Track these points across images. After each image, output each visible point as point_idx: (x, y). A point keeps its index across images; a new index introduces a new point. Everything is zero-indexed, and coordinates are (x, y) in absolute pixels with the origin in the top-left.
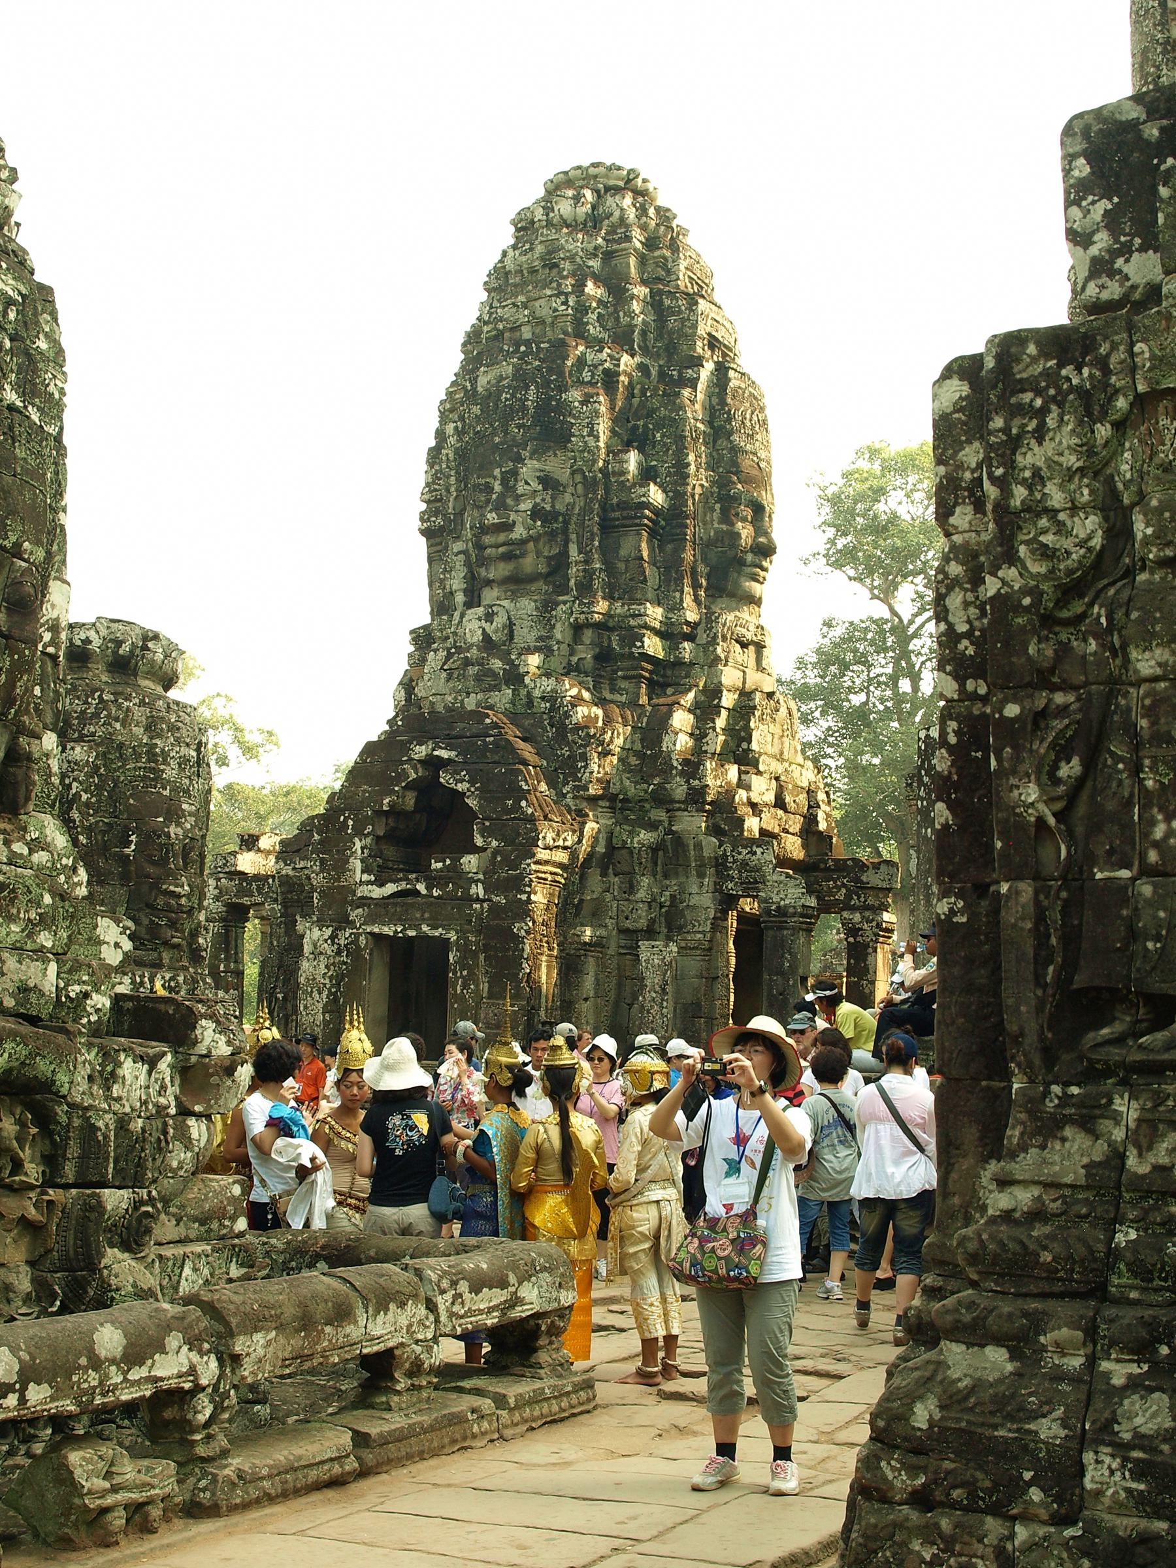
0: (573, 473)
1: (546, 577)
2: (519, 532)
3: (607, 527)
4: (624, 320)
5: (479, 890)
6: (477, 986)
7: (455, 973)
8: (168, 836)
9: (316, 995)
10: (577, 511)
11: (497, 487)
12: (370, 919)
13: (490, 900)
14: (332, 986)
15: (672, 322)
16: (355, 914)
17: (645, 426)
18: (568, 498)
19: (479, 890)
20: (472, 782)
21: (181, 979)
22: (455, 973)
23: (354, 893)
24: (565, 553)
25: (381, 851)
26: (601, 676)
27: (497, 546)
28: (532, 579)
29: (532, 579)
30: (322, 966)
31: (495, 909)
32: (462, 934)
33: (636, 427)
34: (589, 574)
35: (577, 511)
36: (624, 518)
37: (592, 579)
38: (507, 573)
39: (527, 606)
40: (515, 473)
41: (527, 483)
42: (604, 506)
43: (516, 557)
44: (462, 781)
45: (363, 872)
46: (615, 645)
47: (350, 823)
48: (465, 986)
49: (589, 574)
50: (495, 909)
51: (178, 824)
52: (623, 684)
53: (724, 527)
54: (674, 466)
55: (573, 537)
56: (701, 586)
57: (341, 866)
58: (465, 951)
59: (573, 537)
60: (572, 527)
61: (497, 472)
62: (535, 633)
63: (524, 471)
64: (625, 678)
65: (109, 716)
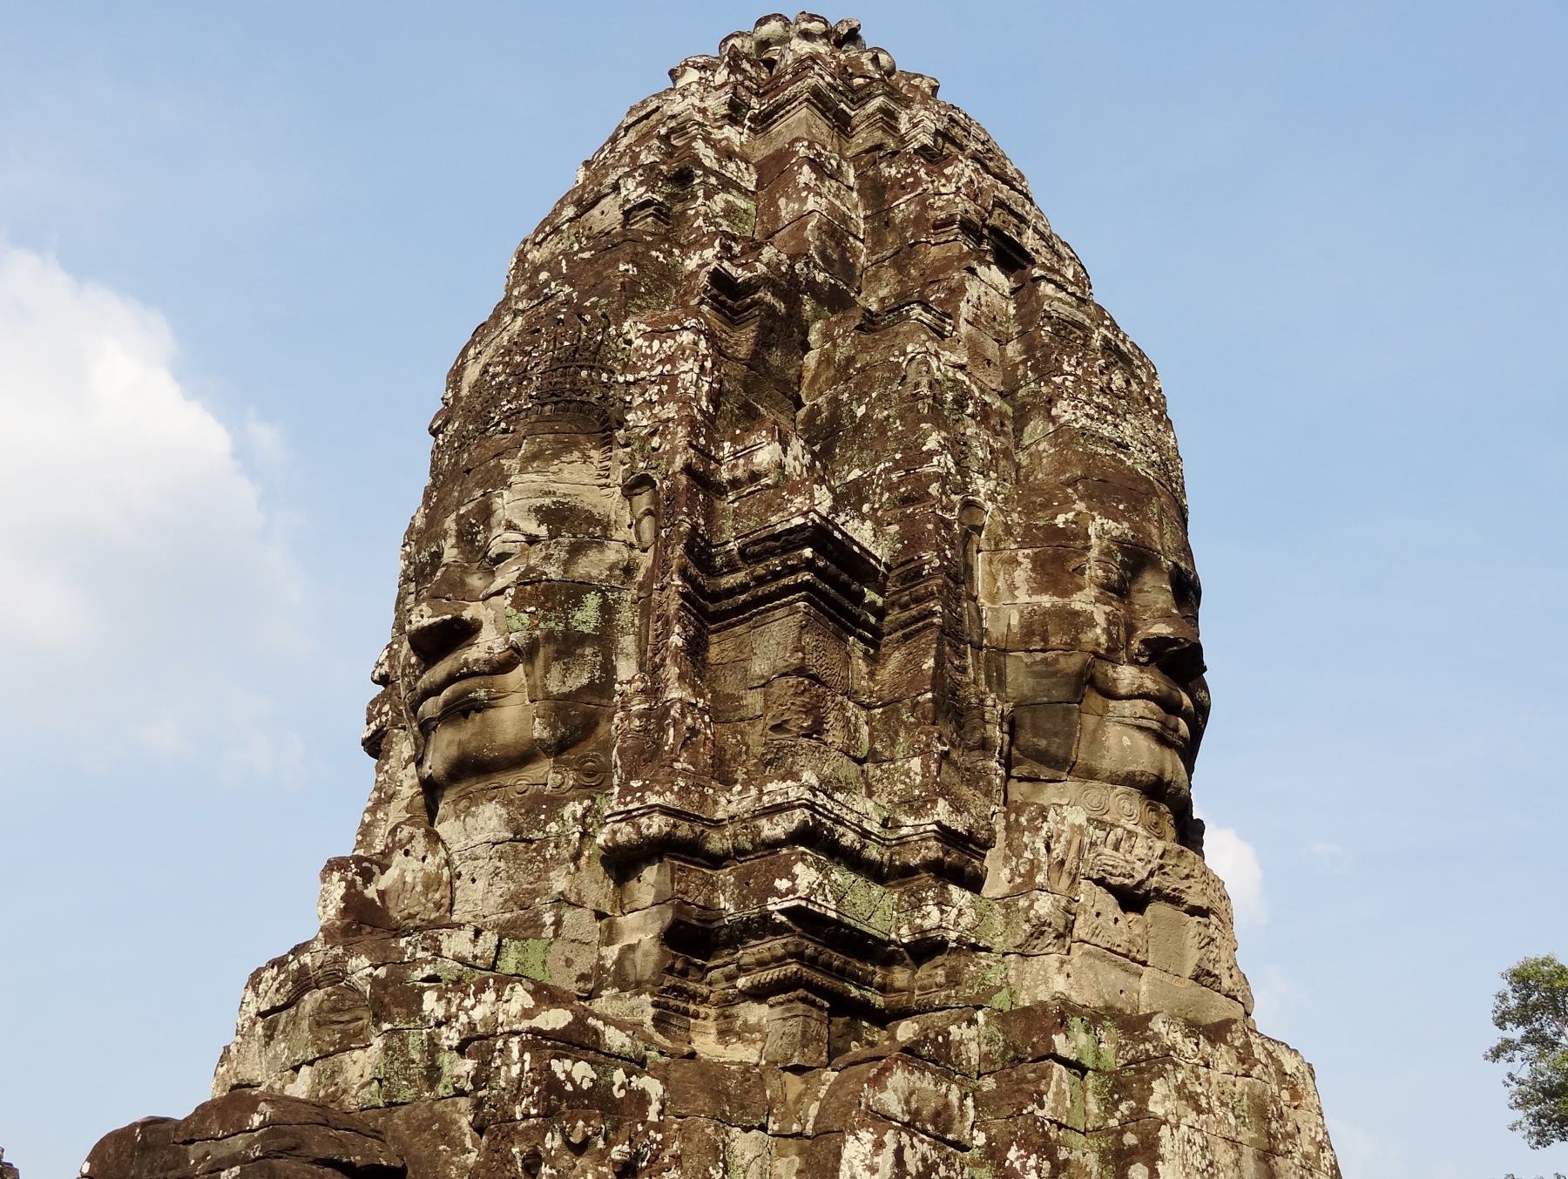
0: (631, 489)
1: (558, 749)
2: (488, 644)
3: (710, 612)
4: (787, 209)
10: (639, 577)
11: (450, 554)
15: (903, 207)
17: (835, 402)
18: (613, 553)
24: (603, 686)
26: (681, 992)
27: (435, 690)
28: (523, 757)
29: (523, 757)
33: (815, 412)
34: (657, 716)
35: (639, 577)
36: (760, 581)
37: (664, 730)
38: (453, 752)
39: (490, 819)
40: (485, 512)
41: (511, 526)
42: (700, 552)
43: (480, 707)
46: (725, 903)
49: (657, 716)
52: (755, 1013)
53: (1046, 600)
54: (897, 466)
55: (628, 643)
56: (985, 746)
59: (628, 643)
60: (626, 615)
61: (450, 523)
62: (502, 887)
63: (507, 505)
64: (758, 994)
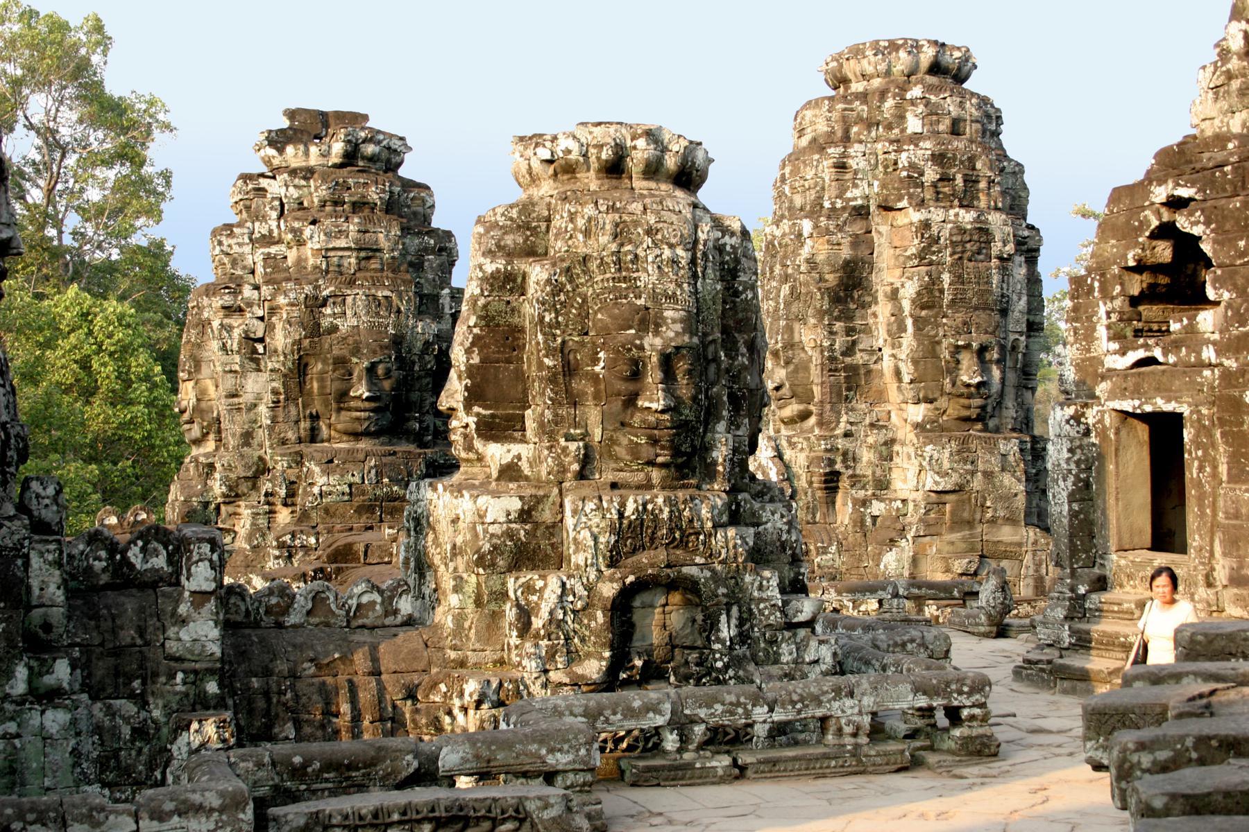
5: (1209, 354)
6: (1215, 468)
7: (1190, 454)
8: (641, 348)
9: (1061, 483)
12: (1112, 395)
13: (1221, 364)
14: (1081, 471)
16: (1102, 389)
19: (1209, 354)
20: (1207, 223)
21: (660, 500)
22: (1190, 454)
23: (1102, 364)
25: (1140, 314)
30: (1065, 450)
31: (1227, 375)
32: (1196, 406)
44: (1197, 223)
45: (1109, 339)
47: (1096, 284)
48: (1201, 469)
50: (1227, 375)
51: (657, 333)
57: (1088, 336)
58: (1201, 428)
65: (574, 229)
